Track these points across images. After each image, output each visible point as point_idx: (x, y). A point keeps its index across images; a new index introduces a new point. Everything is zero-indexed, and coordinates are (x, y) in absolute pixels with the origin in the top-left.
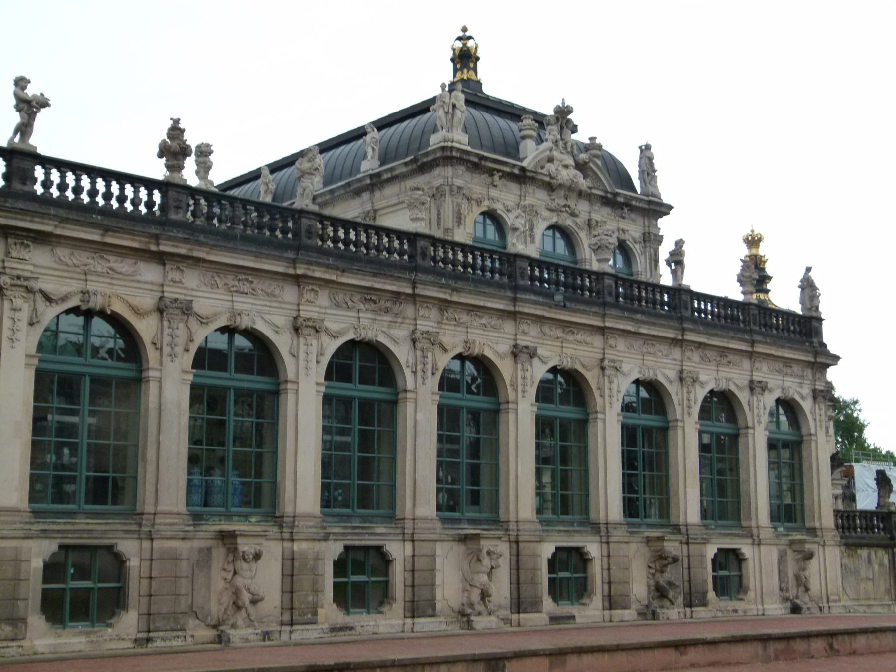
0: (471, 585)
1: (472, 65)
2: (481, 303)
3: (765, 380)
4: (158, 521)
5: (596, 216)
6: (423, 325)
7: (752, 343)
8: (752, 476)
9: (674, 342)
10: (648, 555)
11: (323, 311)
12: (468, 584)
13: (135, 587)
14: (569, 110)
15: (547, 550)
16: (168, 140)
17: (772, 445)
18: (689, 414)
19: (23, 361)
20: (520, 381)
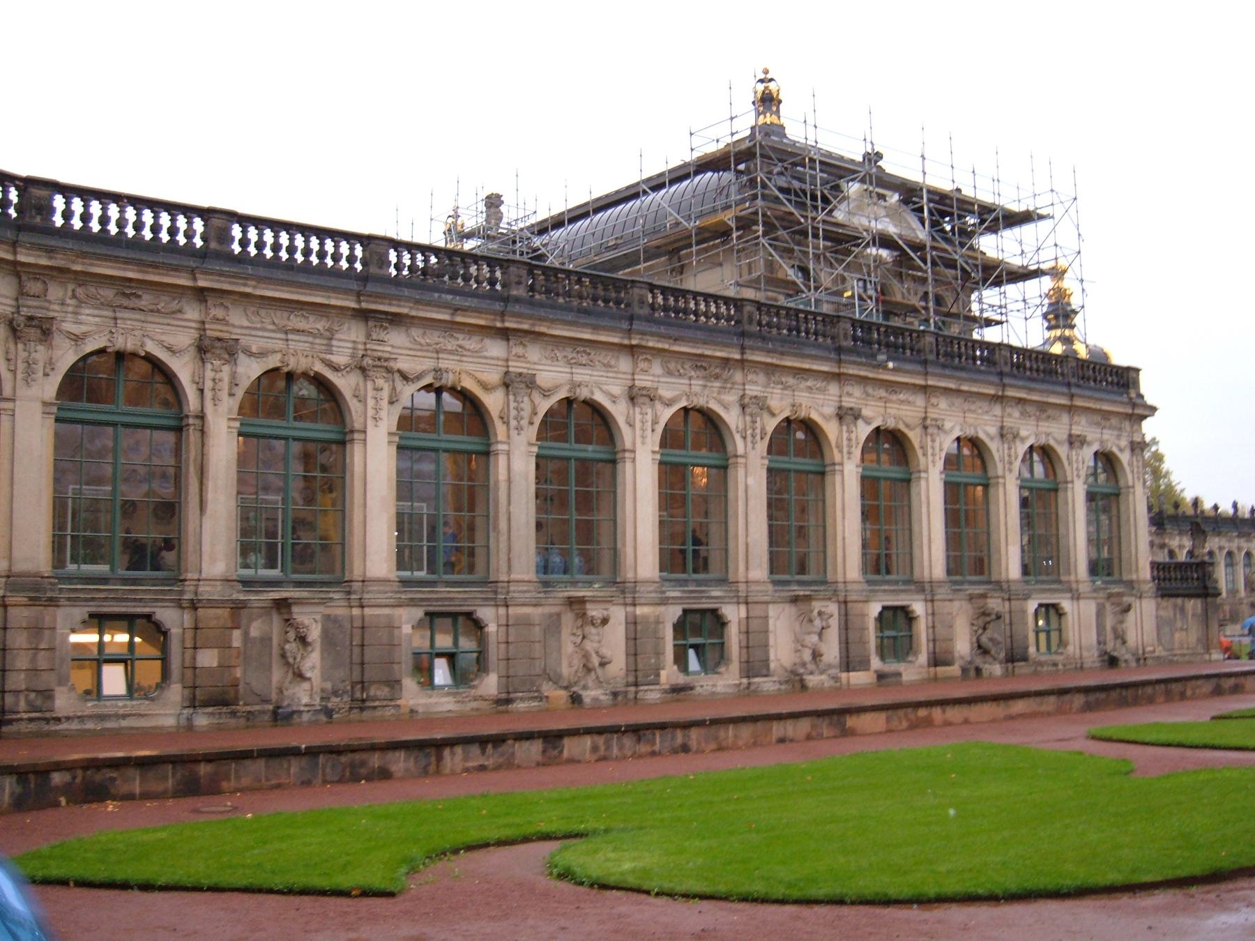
0: (803, 646)
2: (807, 366)
3: (1084, 433)
4: (512, 588)
6: (753, 390)
10: (971, 612)
11: (656, 379)
12: (799, 643)
13: (495, 652)
14: (879, 156)
15: (875, 609)
17: (1091, 497)
18: (1010, 471)
19: (385, 439)
20: (845, 443)
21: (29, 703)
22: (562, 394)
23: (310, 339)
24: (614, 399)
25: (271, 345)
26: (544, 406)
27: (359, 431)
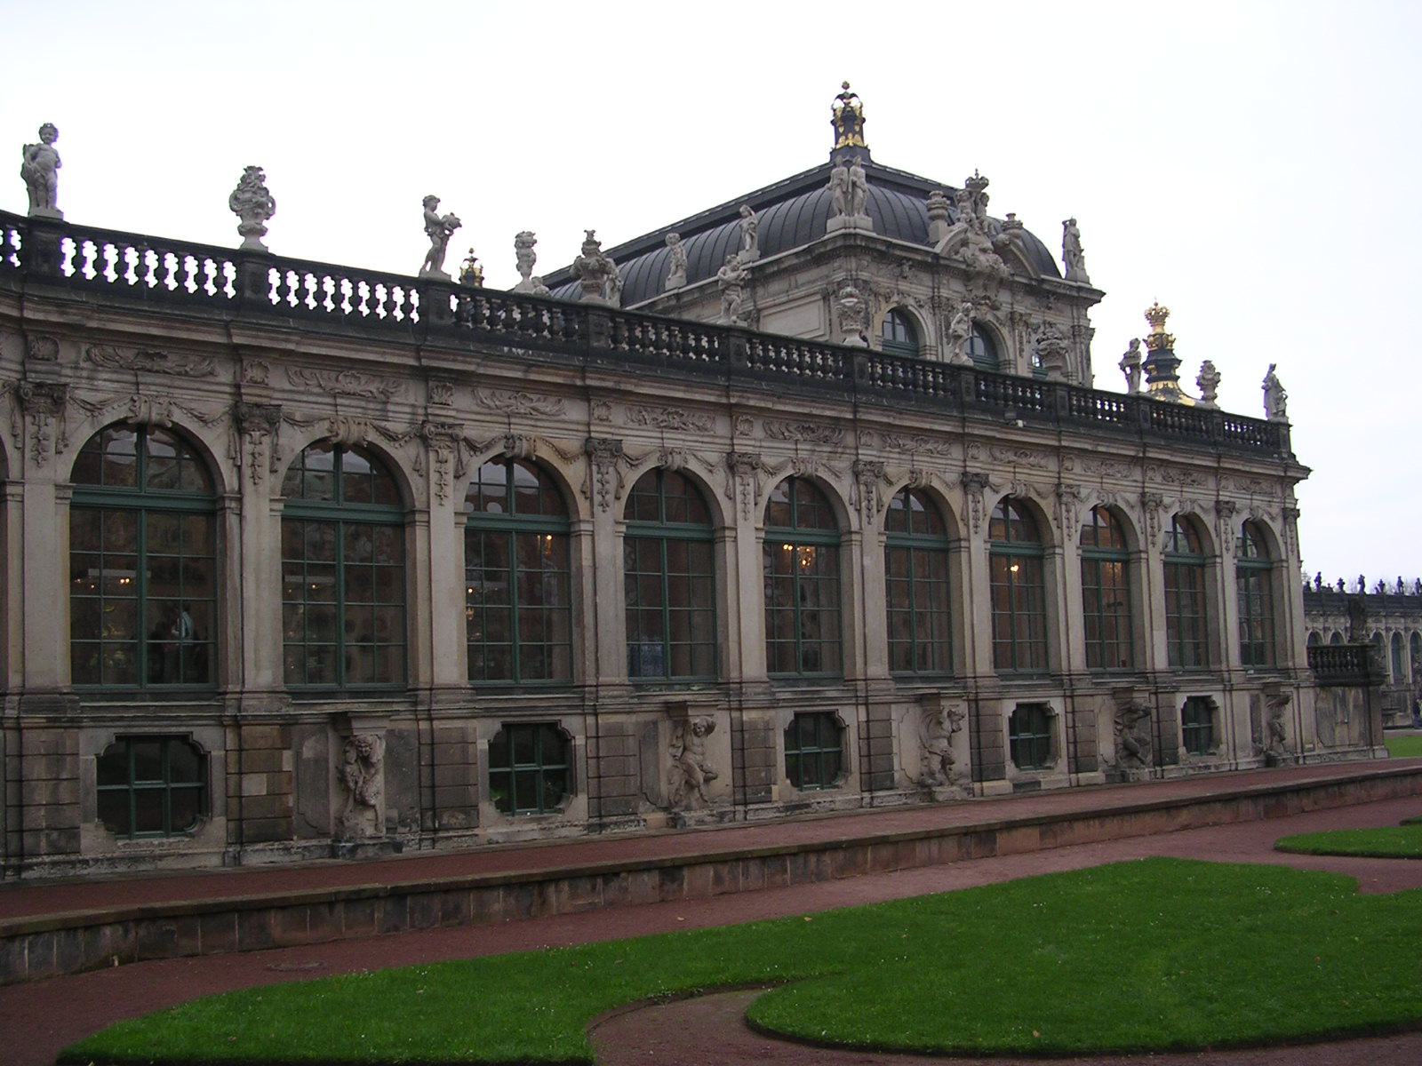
0: (930, 752)
1: (857, 128)
2: (927, 426)
4: (601, 694)
5: (1019, 309)
6: (866, 454)
7: (1219, 458)
8: (1221, 611)
9: (1134, 461)
10: (1114, 708)
11: (758, 444)
12: (926, 749)
13: (583, 768)
15: (1008, 708)
16: (583, 256)
17: (1241, 572)
19: (452, 519)
20: (971, 514)
21: (51, 844)
22: (651, 464)
23: (363, 404)
24: (711, 468)
25: (317, 411)
26: (632, 478)
27: (421, 511)
